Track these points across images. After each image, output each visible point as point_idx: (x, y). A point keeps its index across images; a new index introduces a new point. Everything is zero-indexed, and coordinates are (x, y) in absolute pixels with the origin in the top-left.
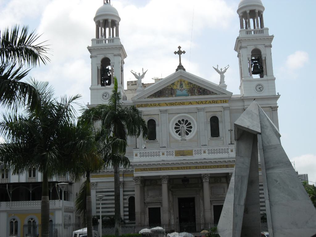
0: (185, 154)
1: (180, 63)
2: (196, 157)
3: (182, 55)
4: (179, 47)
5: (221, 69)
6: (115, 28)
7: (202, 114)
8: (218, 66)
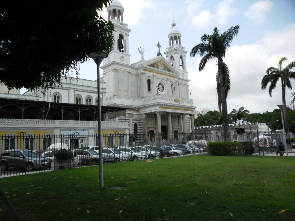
1: (159, 52)
4: (159, 43)
6: (121, 16)
7: (169, 82)
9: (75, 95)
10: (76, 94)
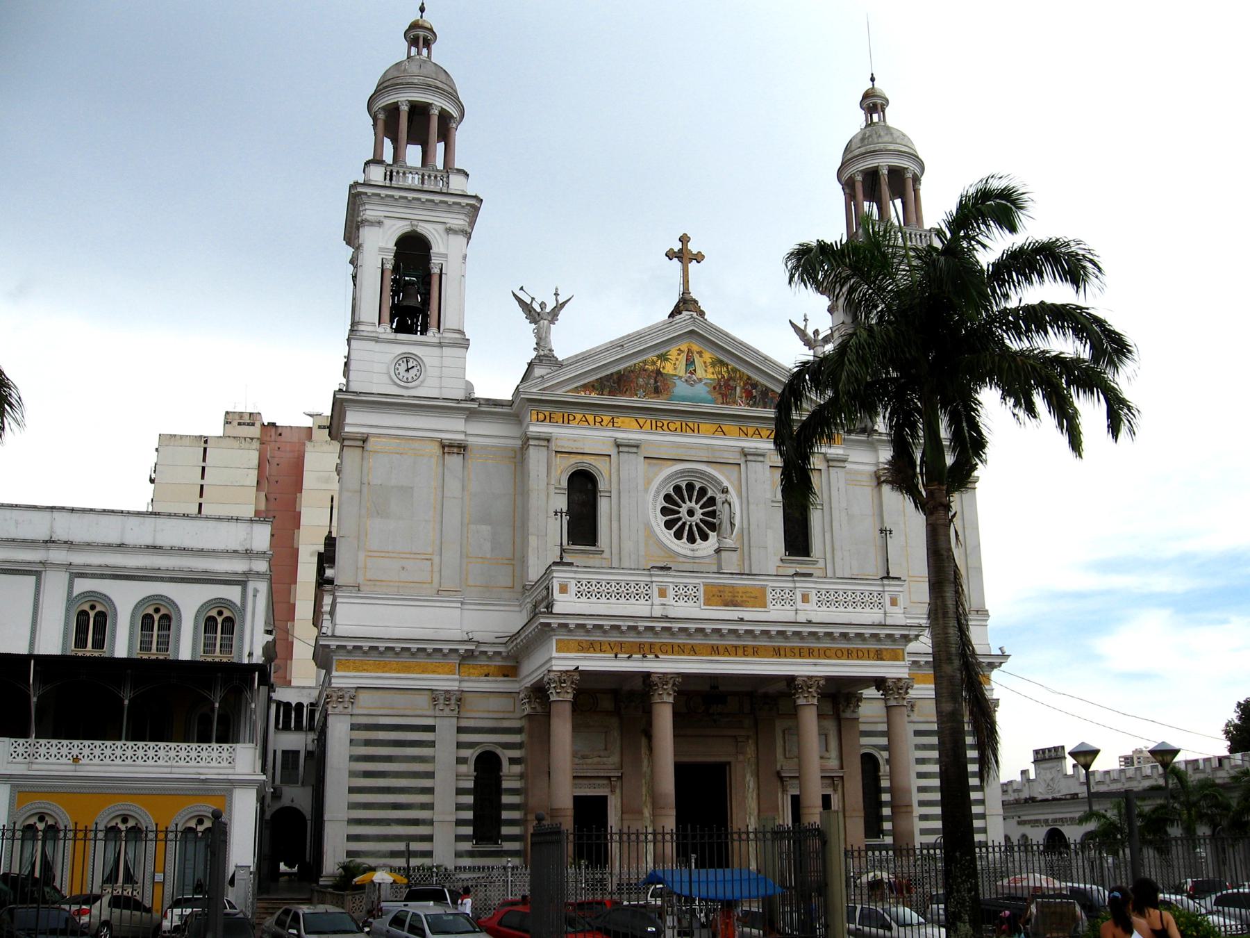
0: (739, 599)
1: (686, 291)
2: (776, 613)
3: (693, 266)
4: (684, 239)
5: (816, 332)
8: (806, 320)
9: (70, 600)
10: (83, 595)
